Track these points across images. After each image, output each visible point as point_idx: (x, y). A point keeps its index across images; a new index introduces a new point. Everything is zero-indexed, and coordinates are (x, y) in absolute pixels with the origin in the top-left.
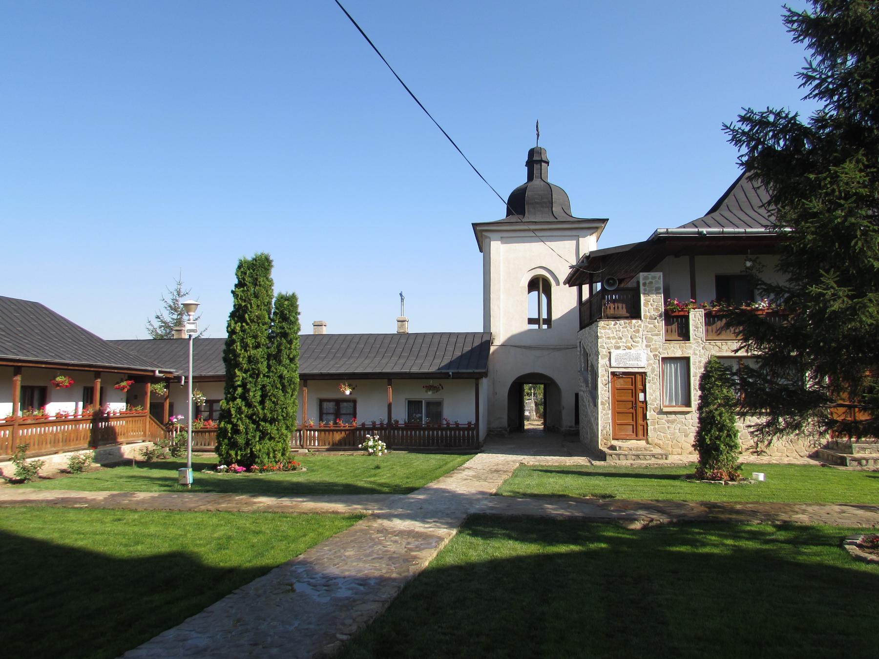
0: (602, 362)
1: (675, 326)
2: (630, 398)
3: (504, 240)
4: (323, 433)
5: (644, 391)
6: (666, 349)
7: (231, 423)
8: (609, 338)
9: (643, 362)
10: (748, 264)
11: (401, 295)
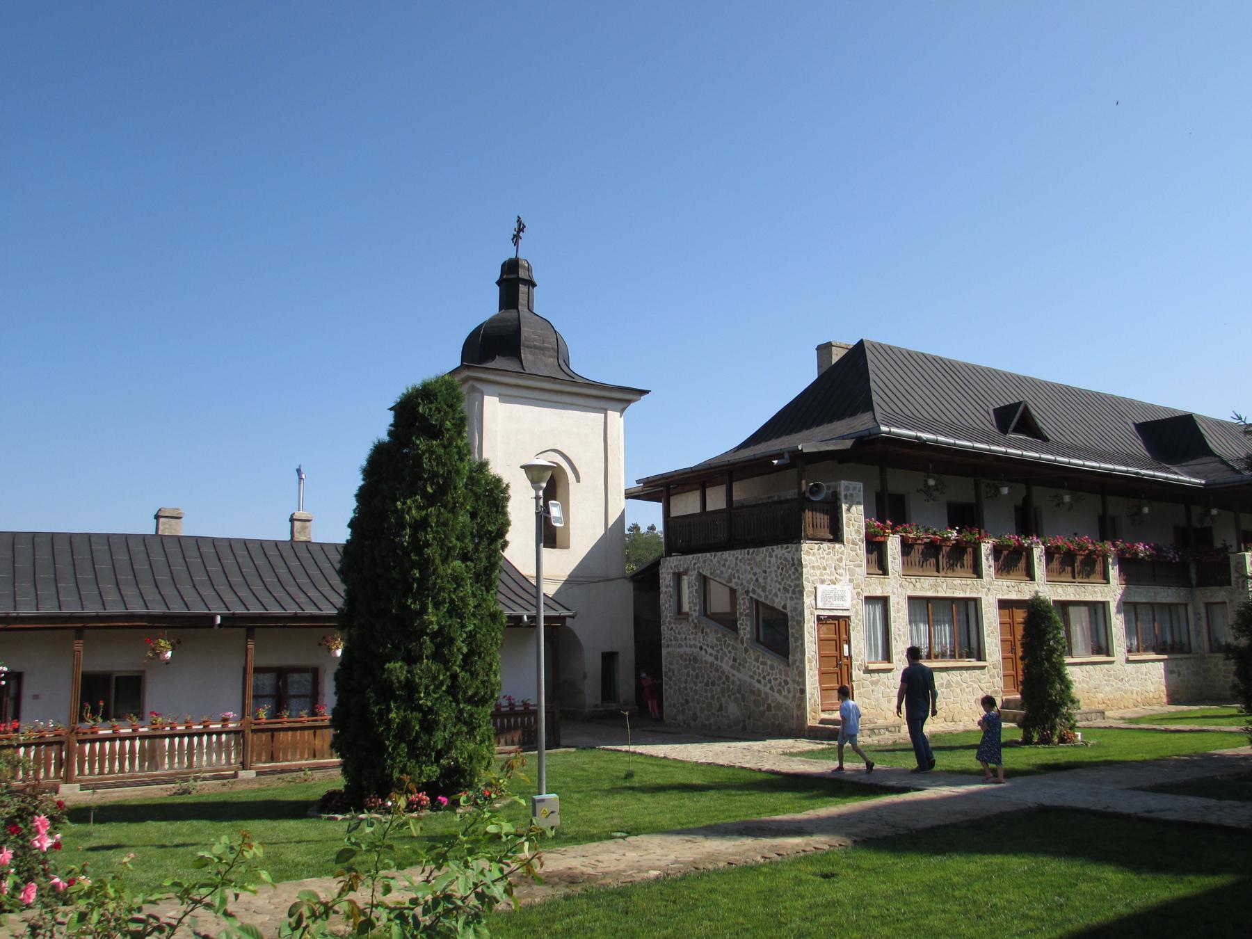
0: (808, 600)
1: (874, 556)
2: (834, 653)
3: (505, 398)
4: (232, 736)
5: (849, 642)
6: (867, 586)
7: (419, 708)
8: (813, 567)
9: (847, 604)
10: (932, 482)
11: (299, 471)
